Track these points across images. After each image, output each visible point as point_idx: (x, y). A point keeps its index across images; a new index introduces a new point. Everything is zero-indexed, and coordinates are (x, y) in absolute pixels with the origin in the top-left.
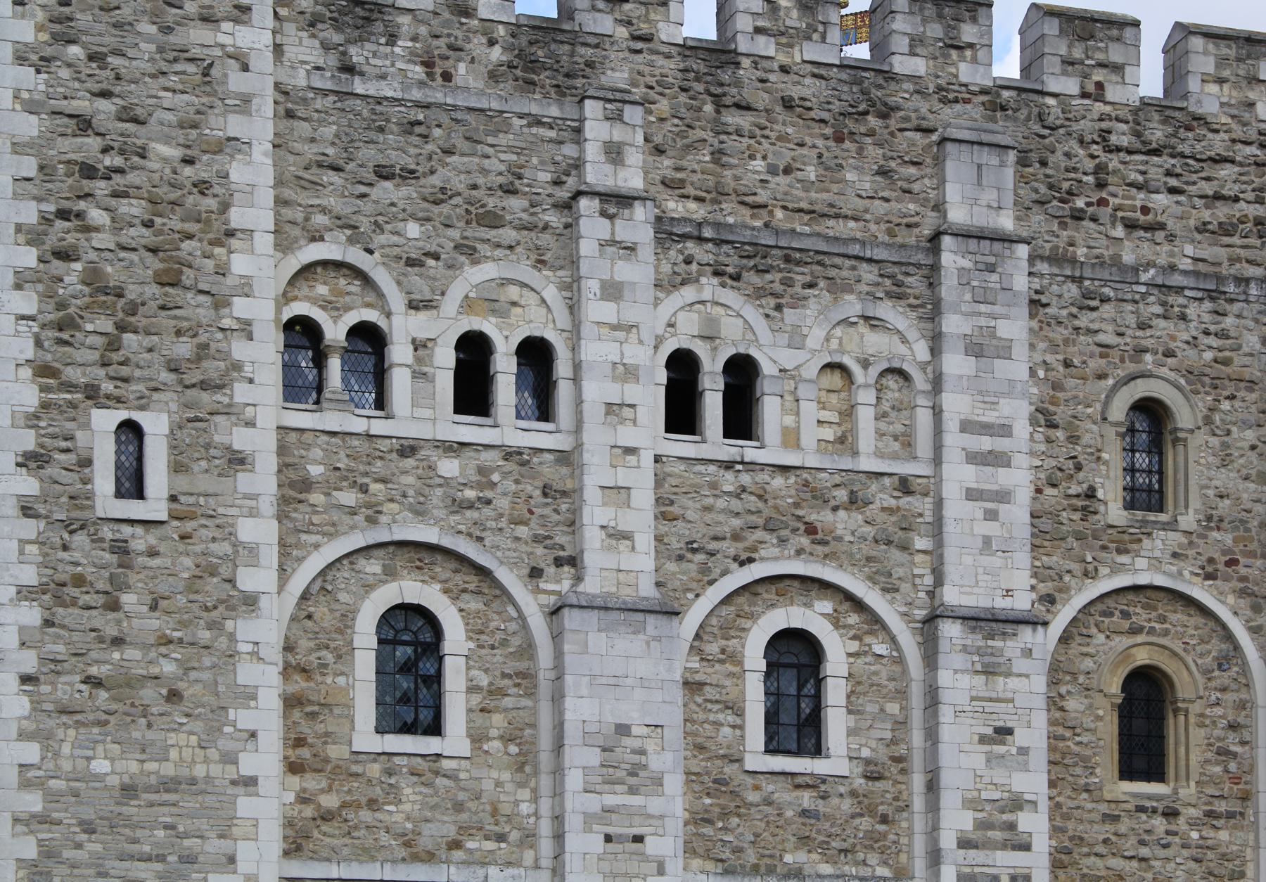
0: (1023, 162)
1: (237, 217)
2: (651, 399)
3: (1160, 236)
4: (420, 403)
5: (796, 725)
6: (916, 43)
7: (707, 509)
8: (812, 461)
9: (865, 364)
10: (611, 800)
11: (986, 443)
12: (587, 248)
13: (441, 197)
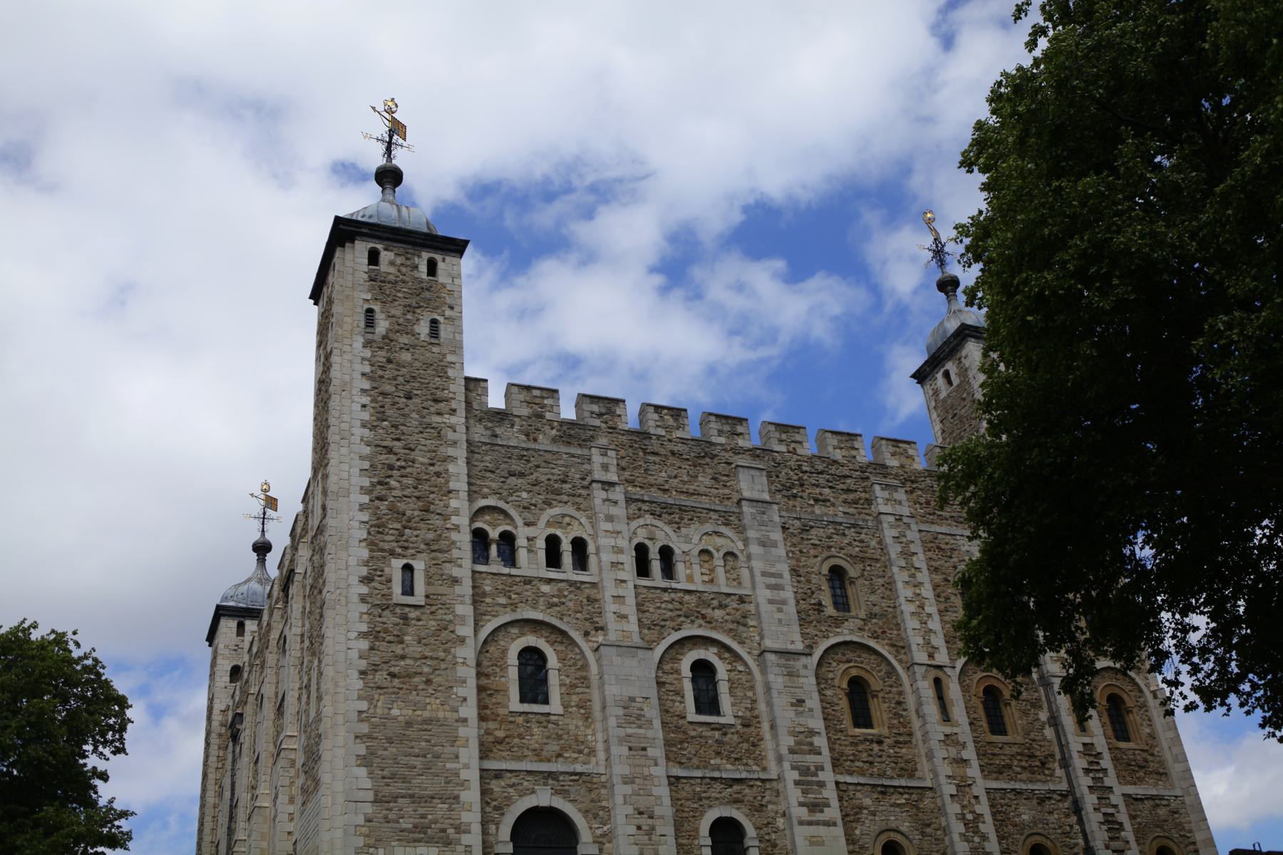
0: (769, 476)
2: (629, 559)
4: (531, 562)
5: (708, 703)
6: (720, 433)
7: (659, 608)
8: (700, 589)
11: (773, 581)
12: (598, 501)
13: (536, 483)
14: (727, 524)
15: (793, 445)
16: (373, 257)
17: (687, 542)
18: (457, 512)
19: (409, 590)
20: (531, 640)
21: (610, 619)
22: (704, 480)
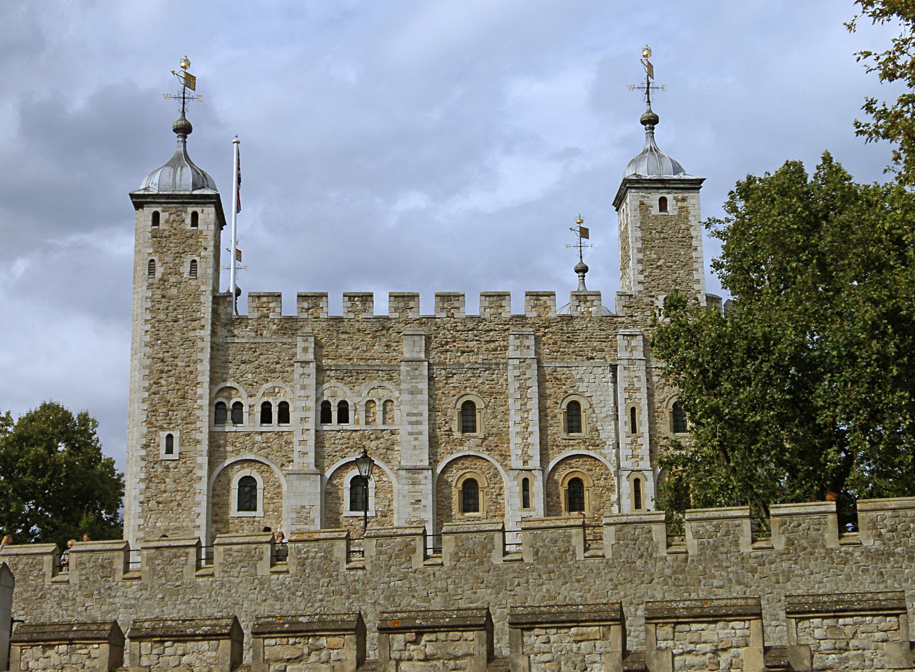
1: (199, 379)
4: (251, 421)
11: (414, 419)
12: (296, 376)
16: (156, 217)
17: (355, 398)
18: (201, 397)
19: (169, 450)
20: (246, 472)
21: (295, 456)
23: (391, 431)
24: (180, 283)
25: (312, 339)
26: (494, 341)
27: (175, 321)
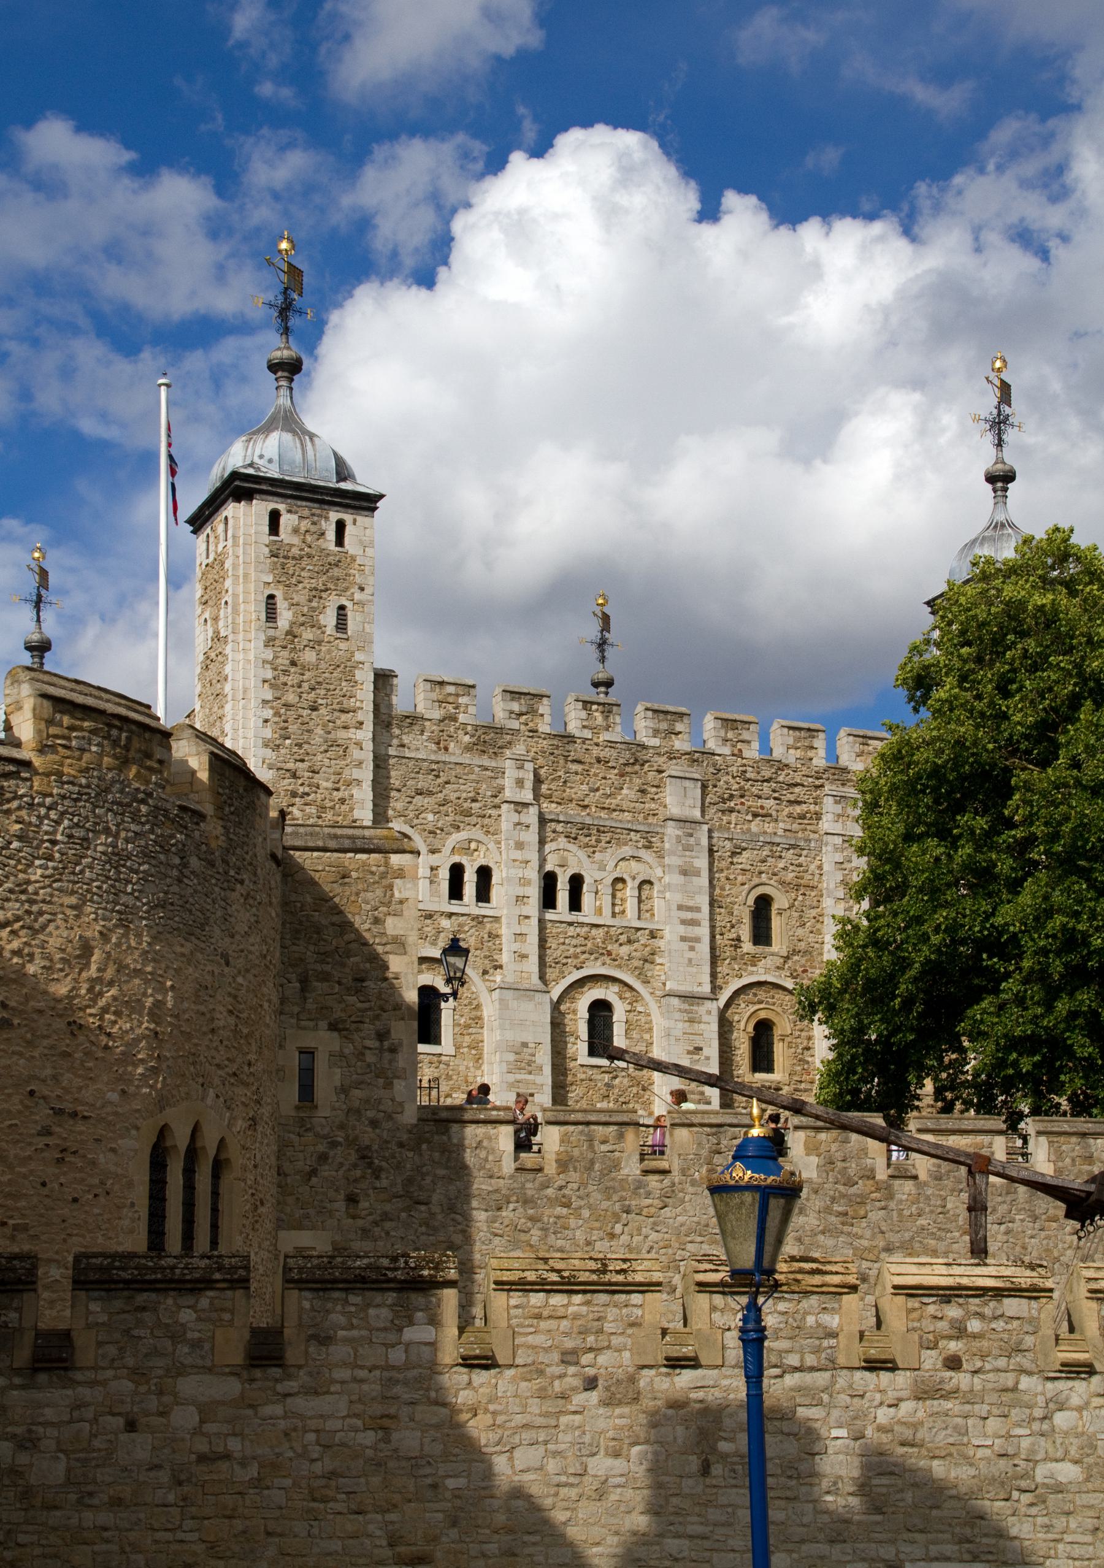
2: (534, 892)
3: (768, 819)
9: (634, 878)
10: (519, 1077)
11: (689, 915)
14: (648, 846)
15: (739, 746)
22: (628, 793)
23: (651, 932)
24: (319, 643)
25: (529, 766)
26: (799, 803)
27: (314, 709)
